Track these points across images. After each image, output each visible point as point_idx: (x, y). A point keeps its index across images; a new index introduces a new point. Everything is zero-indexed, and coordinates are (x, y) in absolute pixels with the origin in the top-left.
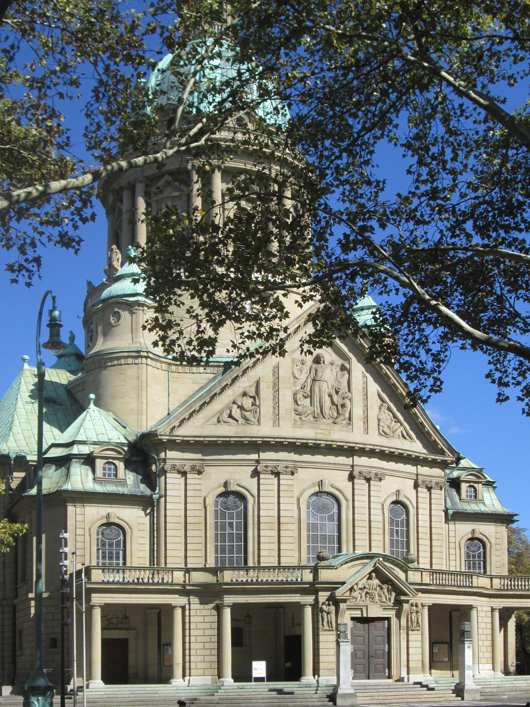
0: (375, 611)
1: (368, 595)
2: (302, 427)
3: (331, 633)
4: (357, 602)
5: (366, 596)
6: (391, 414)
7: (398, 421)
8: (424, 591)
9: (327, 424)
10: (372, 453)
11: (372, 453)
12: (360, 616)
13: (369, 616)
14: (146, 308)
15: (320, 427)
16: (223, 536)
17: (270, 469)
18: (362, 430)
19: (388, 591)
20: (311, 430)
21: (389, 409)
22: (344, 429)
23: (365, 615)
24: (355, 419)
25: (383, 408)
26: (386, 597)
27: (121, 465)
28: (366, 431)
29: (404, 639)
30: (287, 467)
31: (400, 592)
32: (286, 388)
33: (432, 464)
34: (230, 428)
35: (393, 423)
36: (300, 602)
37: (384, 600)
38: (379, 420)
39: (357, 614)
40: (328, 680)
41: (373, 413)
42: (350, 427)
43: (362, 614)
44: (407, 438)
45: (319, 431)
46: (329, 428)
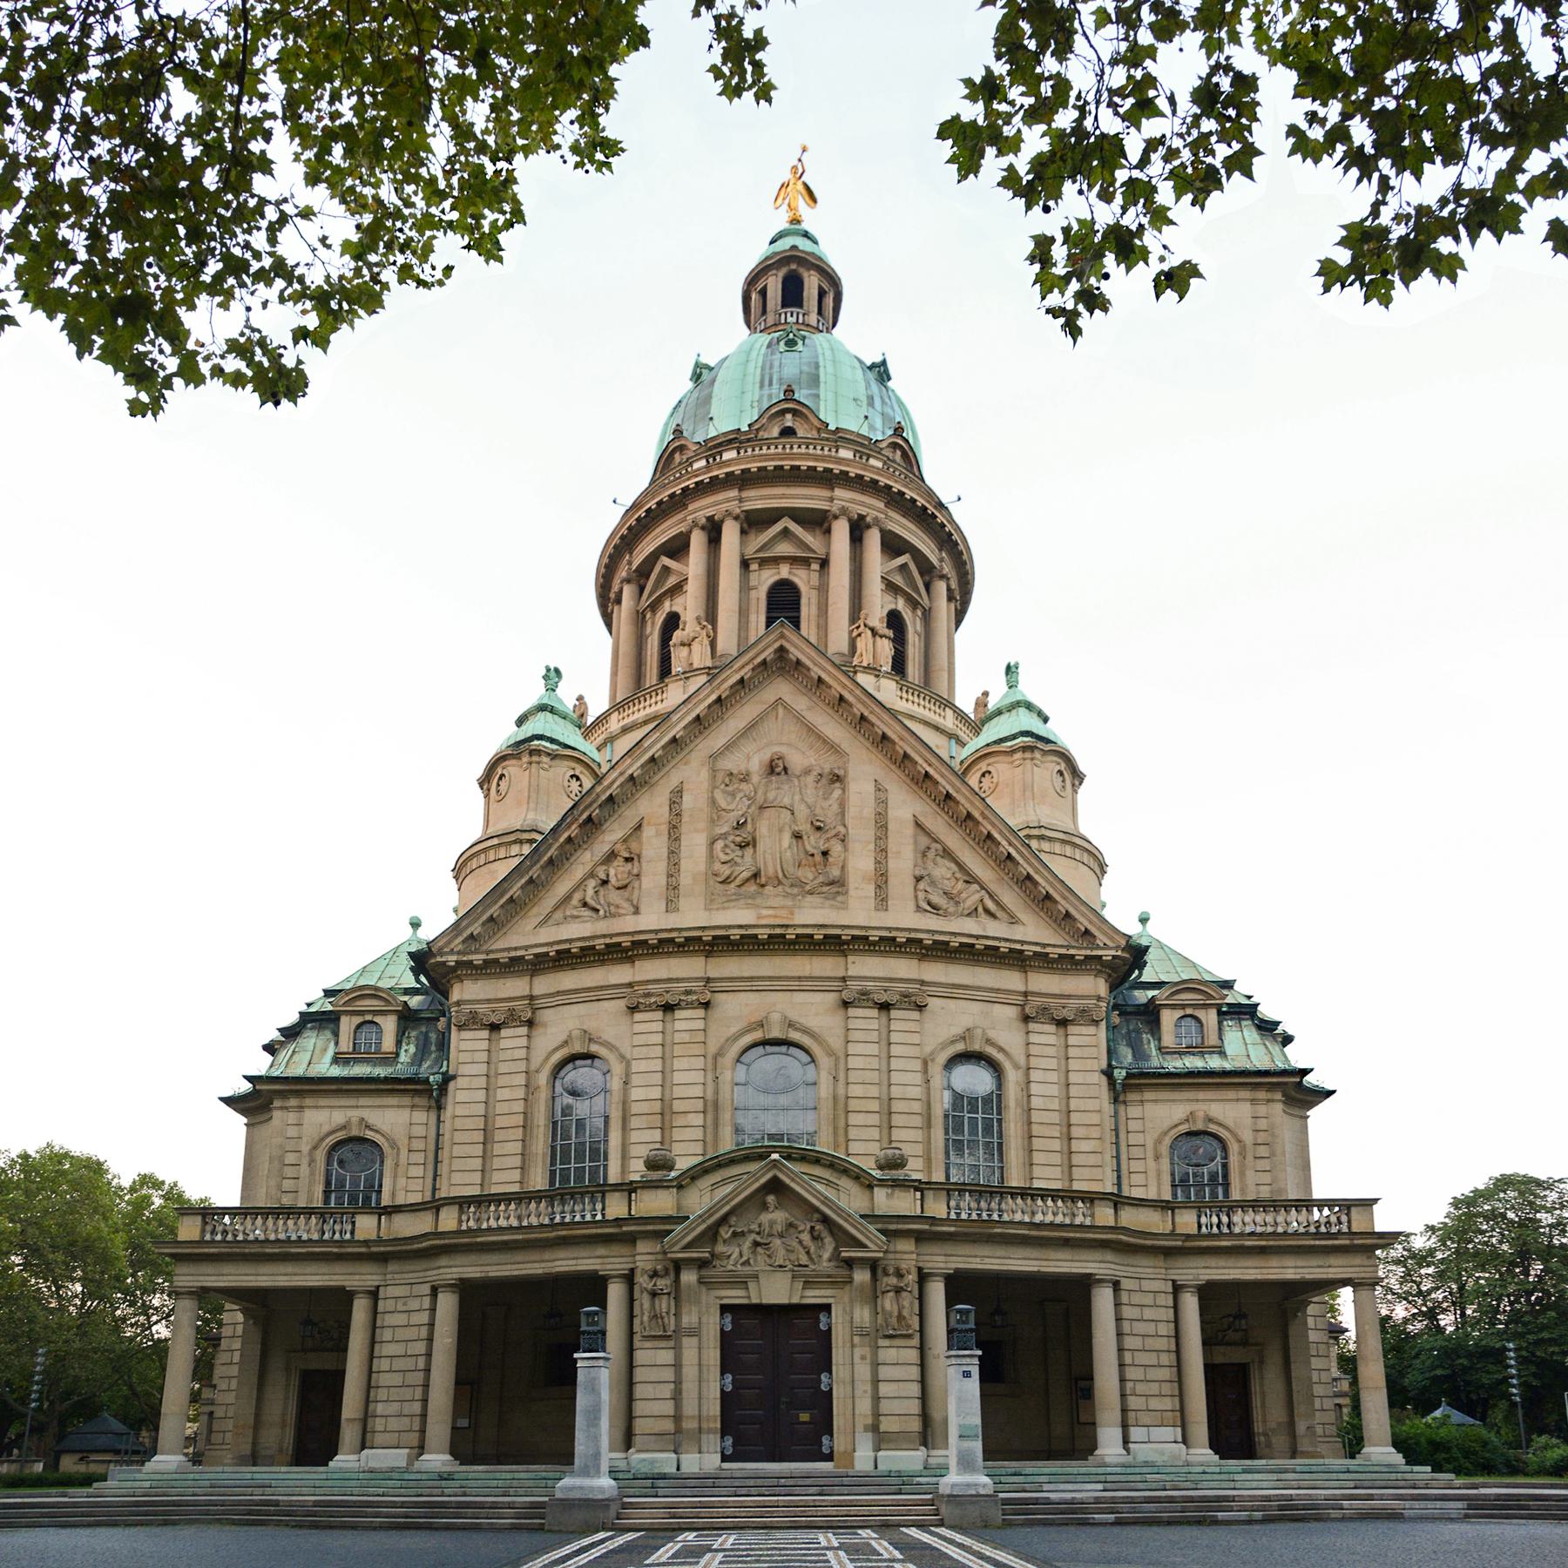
0: (776, 1290)
1: (759, 1249)
2: (724, 908)
3: (663, 1344)
4: (730, 1267)
5: (754, 1252)
6: (953, 866)
7: (971, 879)
8: (920, 1238)
9: (787, 895)
10: (889, 945)
11: (889, 945)
12: (745, 1301)
13: (765, 1301)
14: (545, 759)
15: (768, 904)
16: (566, 1150)
17: (653, 1000)
18: (872, 903)
19: (816, 1238)
20: (746, 911)
21: (947, 853)
22: (828, 903)
23: (755, 1301)
24: (853, 881)
25: (931, 854)
26: (808, 1253)
27: (389, 1025)
28: (882, 901)
29: (863, 1358)
30: (688, 993)
31: (844, 1238)
32: (696, 830)
33: (1066, 964)
34: (581, 925)
35: (960, 885)
36: (596, 1272)
37: (804, 1260)
38: (918, 879)
39: (735, 1296)
40: (653, 1462)
41: (902, 863)
42: (839, 898)
43: (749, 1297)
44: (999, 914)
45: (765, 912)
46: (790, 903)
